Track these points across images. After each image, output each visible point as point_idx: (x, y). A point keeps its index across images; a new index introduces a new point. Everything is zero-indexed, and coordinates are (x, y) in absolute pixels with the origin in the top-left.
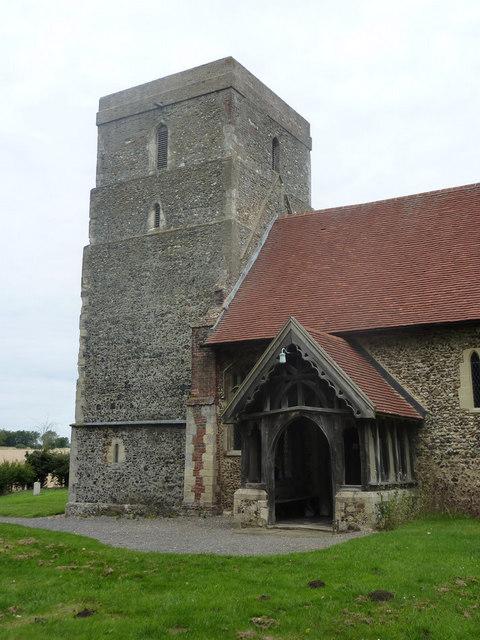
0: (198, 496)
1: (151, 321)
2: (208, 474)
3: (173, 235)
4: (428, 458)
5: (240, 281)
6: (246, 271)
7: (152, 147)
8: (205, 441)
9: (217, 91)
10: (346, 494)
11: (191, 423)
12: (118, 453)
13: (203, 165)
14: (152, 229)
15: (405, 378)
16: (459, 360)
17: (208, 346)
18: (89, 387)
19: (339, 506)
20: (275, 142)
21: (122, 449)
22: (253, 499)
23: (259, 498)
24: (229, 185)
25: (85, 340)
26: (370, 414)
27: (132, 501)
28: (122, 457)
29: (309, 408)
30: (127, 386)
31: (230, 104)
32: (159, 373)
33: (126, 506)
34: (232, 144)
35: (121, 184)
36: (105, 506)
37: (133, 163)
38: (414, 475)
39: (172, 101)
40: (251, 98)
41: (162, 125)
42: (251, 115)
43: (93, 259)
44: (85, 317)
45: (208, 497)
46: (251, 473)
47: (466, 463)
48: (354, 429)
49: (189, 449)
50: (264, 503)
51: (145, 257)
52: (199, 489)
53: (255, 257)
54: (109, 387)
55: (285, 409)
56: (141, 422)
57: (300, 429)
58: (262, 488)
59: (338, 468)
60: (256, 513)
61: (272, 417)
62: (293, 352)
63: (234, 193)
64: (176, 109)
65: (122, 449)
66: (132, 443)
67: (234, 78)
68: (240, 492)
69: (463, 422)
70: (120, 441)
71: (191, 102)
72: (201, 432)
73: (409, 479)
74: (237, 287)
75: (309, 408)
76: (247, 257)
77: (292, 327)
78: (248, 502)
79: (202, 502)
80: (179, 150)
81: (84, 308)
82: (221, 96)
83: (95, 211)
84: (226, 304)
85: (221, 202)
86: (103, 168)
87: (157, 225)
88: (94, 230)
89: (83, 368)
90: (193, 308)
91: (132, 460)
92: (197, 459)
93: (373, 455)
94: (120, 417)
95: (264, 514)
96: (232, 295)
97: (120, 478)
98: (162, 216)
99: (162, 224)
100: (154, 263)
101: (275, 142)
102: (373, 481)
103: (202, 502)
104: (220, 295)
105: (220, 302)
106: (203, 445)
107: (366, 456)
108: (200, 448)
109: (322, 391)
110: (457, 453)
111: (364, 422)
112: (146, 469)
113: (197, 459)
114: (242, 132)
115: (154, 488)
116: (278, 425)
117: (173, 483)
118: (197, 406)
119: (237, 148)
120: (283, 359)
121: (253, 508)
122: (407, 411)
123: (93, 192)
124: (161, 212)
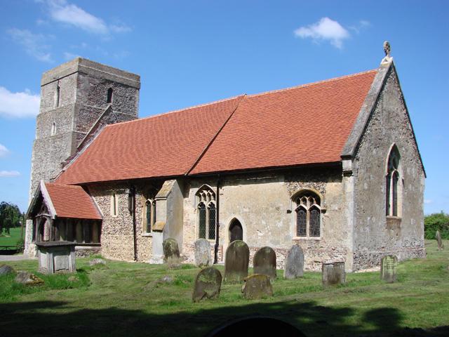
7: (55, 97)
14: (52, 134)
100: (51, 149)
109: (45, 209)
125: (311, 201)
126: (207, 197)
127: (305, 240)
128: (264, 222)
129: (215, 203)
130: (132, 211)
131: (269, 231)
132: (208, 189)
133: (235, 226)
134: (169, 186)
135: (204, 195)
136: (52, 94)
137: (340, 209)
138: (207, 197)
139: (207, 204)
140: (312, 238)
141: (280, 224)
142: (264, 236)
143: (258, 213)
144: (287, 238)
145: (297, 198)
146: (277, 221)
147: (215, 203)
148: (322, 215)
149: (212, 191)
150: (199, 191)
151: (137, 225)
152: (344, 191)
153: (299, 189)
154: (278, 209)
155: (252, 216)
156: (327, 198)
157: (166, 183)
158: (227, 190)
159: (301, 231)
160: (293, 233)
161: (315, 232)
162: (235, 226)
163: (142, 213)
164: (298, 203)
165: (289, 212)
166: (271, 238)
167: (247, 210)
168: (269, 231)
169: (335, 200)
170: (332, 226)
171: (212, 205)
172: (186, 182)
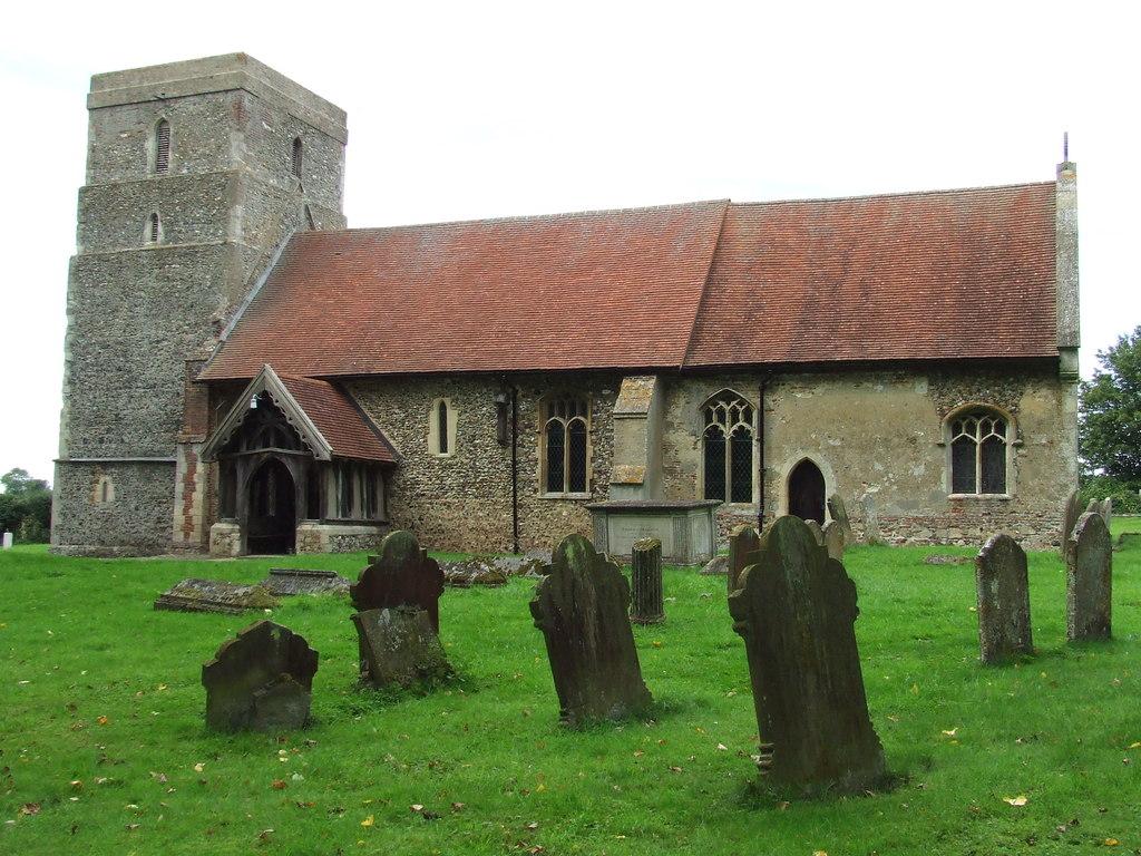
0: (187, 535)
1: (145, 348)
2: (197, 512)
4: (400, 499)
5: (243, 309)
6: (250, 298)
7: (150, 145)
8: (196, 480)
9: (227, 91)
10: (306, 527)
11: (181, 460)
12: (107, 490)
13: (207, 175)
14: (148, 244)
15: (384, 422)
16: (429, 408)
17: (202, 381)
18: (77, 418)
19: (299, 537)
21: (111, 487)
22: (227, 531)
23: (233, 531)
24: (234, 202)
25: (70, 364)
26: (327, 456)
27: (122, 543)
28: (111, 496)
29: (279, 450)
30: (118, 418)
31: (239, 107)
32: (152, 406)
33: (115, 549)
34: (237, 154)
35: (115, 186)
36: (93, 548)
37: (129, 162)
38: (386, 514)
39: (176, 94)
40: (267, 97)
41: (163, 121)
42: (266, 117)
43: (80, 270)
44: (70, 338)
45: (196, 537)
46: (227, 510)
47: (431, 503)
48: (315, 469)
49: (180, 487)
50: (237, 535)
51: (140, 274)
52: (188, 527)
53: (261, 282)
54: (98, 419)
55: (259, 450)
56: (131, 459)
57: (275, 464)
58: (236, 523)
59: (301, 504)
60: (229, 544)
61: (247, 458)
62: (266, 399)
63: (239, 210)
64: (181, 103)
65: (111, 487)
66: (121, 481)
67: (245, 78)
68: (217, 525)
69: (430, 466)
70: (108, 478)
71: (197, 99)
72: (192, 470)
73: (380, 516)
74: (238, 316)
75: (279, 450)
76: (252, 282)
77: (266, 375)
78: (222, 535)
79: (190, 540)
80: (183, 153)
81: (70, 328)
82: (230, 97)
83: (84, 214)
84: (223, 336)
85: (223, 219)
86: (93, 163)
87: (154, 238)
88: (83, 238)
89: (69, 397)
90: (191, 336)
91: (122, 499)
92: (187, 497)
93: (333, 494)
94: (111, 452)
95: (237, 547)
96: (232, 325)
97: (108, 518)
98: (160, 229)
99: (161, 238)
100: (150, 281)
101: (297, 143)
102: (332, 513)
103: (190, 540)
105: (217, 333)
106: (194, 484)
107: (325, 494)
108: (190, 485)
109: (289, 435)
110: (424, 495)
111: (324, 463)
112: (137, 509)
113: (187, 497)
115: (144, 530)
116: (252, 465)
117: (163, 523)
118: (188, 444)
119: (247, 158)
120: (254, 405)
121: (227, 540)
122: (377, 454)
123: (83, 191)
124: (160, 224)
125: (986, 429)
126: (728, 418)
127: (977, 500)
128: (879, 467)
129: (754, 430)
130: (509, 437)
131: (891, 484)
132: (728, 397)
133: (806, 479)
134: (637, 394)
136: (137, 140)
138: (728, 418)
139: (728, 431)
140: (989, 495)
141: (919, 471)
142: (879, 493)
143: (866, 447)
144: (935, 497)
145: (955, 425)
146: (911, 464)
148: (1009, 454)
150: (713, 402)
151: (521, 475)
153: (961, 404)
154: (913, 440)
157: (626, 383)
159: (961, 482)
160: (945, 483)
161: (994, 482)
162: (806, 479)
163: (536, 449)
164: (956, 429)
165: (942, 446)
166: (897, 498)
167: (838, 443)
168: (891, 484)
170: (1036, 474)
172: (671, 380)
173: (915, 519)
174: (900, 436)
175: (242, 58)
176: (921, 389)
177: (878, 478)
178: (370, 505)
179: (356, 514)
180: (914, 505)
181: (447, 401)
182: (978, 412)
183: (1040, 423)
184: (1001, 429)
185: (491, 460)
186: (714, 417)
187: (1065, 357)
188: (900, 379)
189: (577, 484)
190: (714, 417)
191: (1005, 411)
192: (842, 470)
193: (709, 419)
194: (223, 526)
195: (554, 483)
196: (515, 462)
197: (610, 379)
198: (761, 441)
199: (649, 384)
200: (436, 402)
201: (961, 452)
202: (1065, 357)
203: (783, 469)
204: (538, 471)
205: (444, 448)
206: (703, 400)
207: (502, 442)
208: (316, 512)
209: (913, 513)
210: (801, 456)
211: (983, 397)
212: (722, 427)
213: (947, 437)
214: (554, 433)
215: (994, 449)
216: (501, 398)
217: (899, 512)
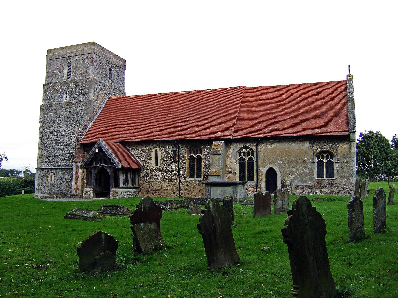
0: (76, 192)
1: (64, 133)
2: (79, 184)
3: (71, 103)
4: (143, 180)
5: (93, 121)
6: (96, 117)
7: (66, 71)
8: (79, 174)
9: (89, 54)
10: (113, 189)
11: (74, 168)
12: (52, 177)
13: (82, 79)
14: (64, 101)
15: (138, 156)
16: (152, 152)
17: (81, 144)
18: (41, 155)
19: (111, 192)
20: (110, 69)
21: (53, 176)
23: (90, 191)
24: (91, 88)
25: (41, 138)
26: (120, 167)
27: (56, 194)
28: (53, 179)
29: (105, 165)
30: (55, 155)
31: (92, 58)
32: (65, 151)
33: (54, 195)
35: (54, 83)
36: (48, 195)
37: (59, 76)
38: (139, 185)
39: (73, 55)
40: (101, 55)
41: (69, 63)
42: (100, 62)
43: (43, 109)
44: (41, 130)
45: (79, 192)
46: (88, 184)
47: (153, 181)
48: (116, 171)
49: (74, 177)
50: (92, 192)
51: (62, 111)
52: (77, 189)
53: (99, 112)
54: (49, 155)
55: (99, 165)
56: (59, 168)
57: (103, 170)
58: (91, 188)
59: (112, 182)
60: (89, 195)
61: (95, 168)
62: (101, 149)
63: (93, 90)
64: (75, 58)
65: (53, 176)
66: (56, 174)
67: (94, 49)
68: (85, 189)
70: (52, 174)
71: (79, 56)
72: (78, 171)
73: (137, 186)
74: (92, 123)
75: (105, 165)
76: (96, 113)
77: (101, 141)
78: (87, 192)
79: (77, 193)
80: (75, 73)
81: (41, 127)
83: (45, 92)
84: (87, 129)
86: (47, 77)
87: (66, 99)
88: (44, 99)
89: (40, 149)
90: (77, 130)
91: (56, 180)
92: (76, 180)
93: (122, 179)
94: (53, 165)
96: (90, 126)
97: (53, 186)
98: (68, 96)
99: (68, 99)
101: (110, 69)
102: (122, 185)
103: (77, 193)
104: (86, 126)
105: (86, 128)
106: (78, 175)
107: (119, 179)
108: (77, 176)
109: (108, 160)
110: (150, 179)
111: (119, 169)
112: (61, 183)
113: (76, 180)
114: (97, 68)
115: (64, 189)
116: (96, 170)
117: (70, 187)
118: (76, 163)
120: (97, 151)
121: (89, 193)
124: (68, 95)
125: (327, 157)
126: (246, 154)
127: (325, 180)
128: (294, 170)
131: (298, 175)
132: (246, 148)
133: (271, 174)
135: (244, 153)
136: (61, 69)
137: (348, 162)
138: (246, 154)
139: (246, 158)
141: (307, 171)
142: (294, 178)
143: (289, 164)
144: (312, 179)
147: (254, 158)
149: (251, 149)
150: (241, 149)
151: (181, 173)
152: (350, 152)
153: (319, 150)
154: (305, 161)
155: (285, 166)
156: (339, 155)
157: (214, 143)
158: (264, 147)
159: (320, 174)
160: (315, 175)
161: (330, 174)
162: (271, 174)
164: (318, 158)
166: (300, 179)
167: (281, 162)
168: (298, 175)
169: (344, 157)
170: (343, 172)
171: (251, 159)
173: (306, 186)
174: (300, 160)
175: (93, 43)
176: (307, 144)
177: (294, 173)
178: (133, 182)
179: (129, 185)
180: (305, 181)
181: (158, 149)
182: (325, 152)
183: (344, 155)
184: (332, 158)
185: (171, 167)
186: (242, 154)
187: (351, 134)
188: (300, 142)
189: (199, 176)
190: (242, 154)
191: (333, 152)
192: (282, 171)
193: (240, 155)
194: (88, 189)
195: (192, 176)
196: (179, 169)
197: (210, 142)
198: (257, 161)
199: (222, 143)
200: (154, 150)
201: (320, 164)
202: (351, 134)
203: (264, 170)
204: (186, 171)
205: (157, 164)
206: (238, 149)
207: (175, 162)
208: (117, 185)
209: (305, 184)
210: (269, 166)
211: (327, 147)
212: (244, 157)
213: (316, 160)
214: (192, 158)
215: (330, 164)
216: (175, 149)
217: (300, 183)
